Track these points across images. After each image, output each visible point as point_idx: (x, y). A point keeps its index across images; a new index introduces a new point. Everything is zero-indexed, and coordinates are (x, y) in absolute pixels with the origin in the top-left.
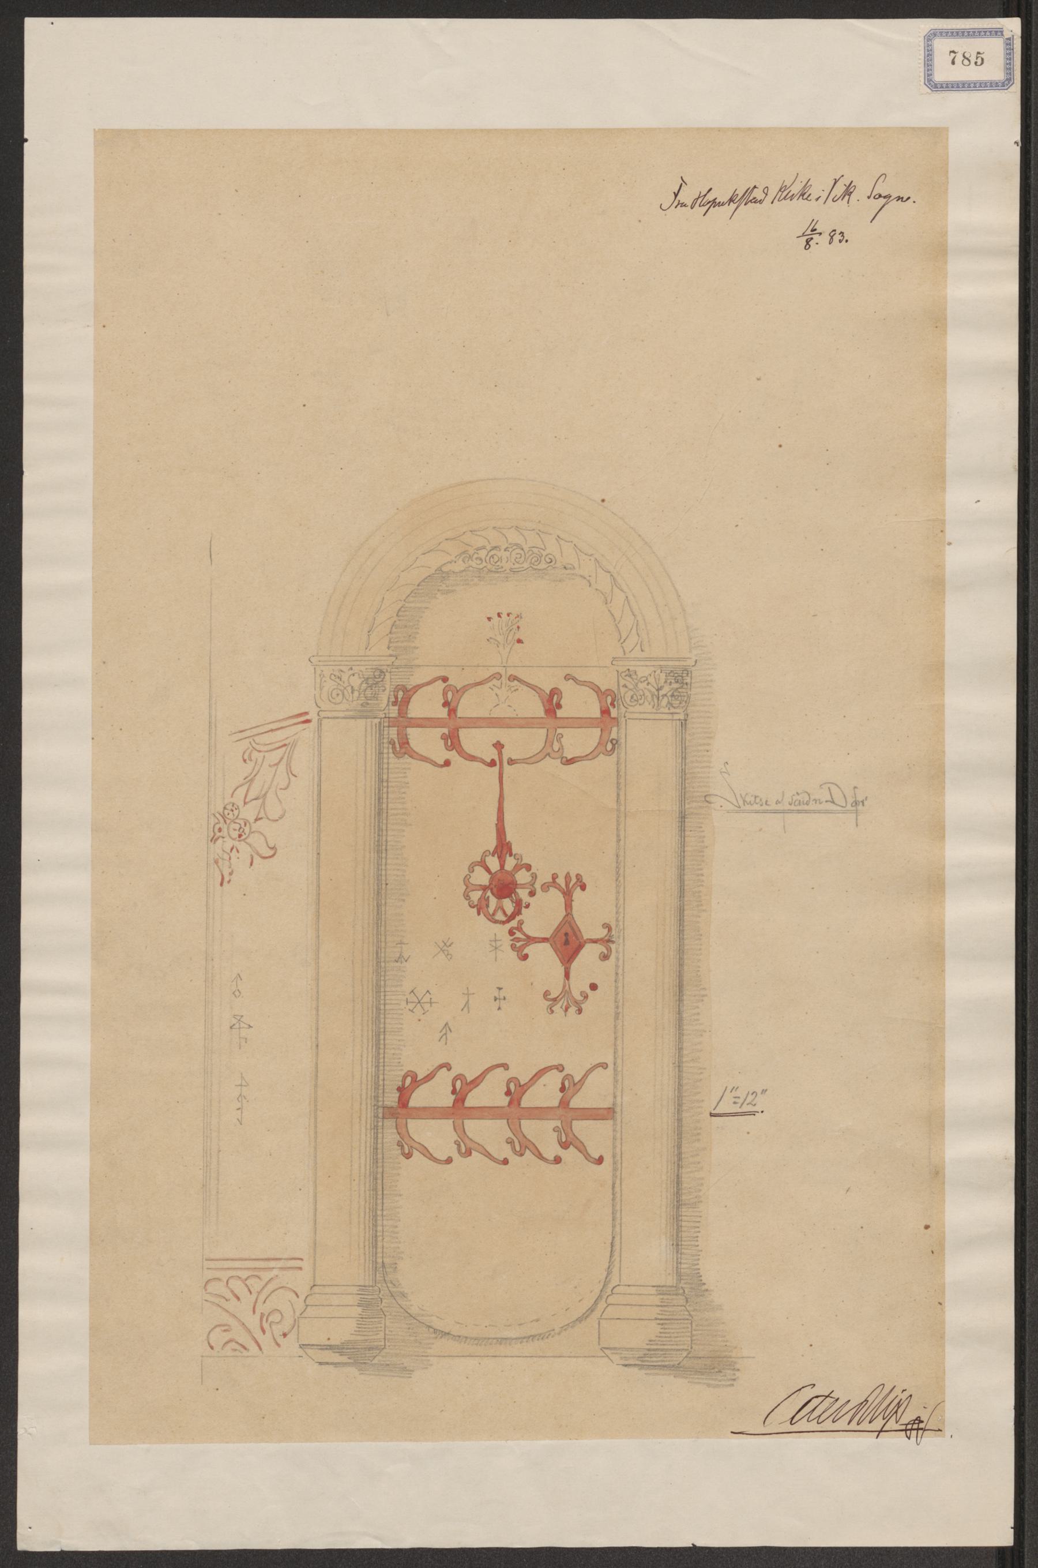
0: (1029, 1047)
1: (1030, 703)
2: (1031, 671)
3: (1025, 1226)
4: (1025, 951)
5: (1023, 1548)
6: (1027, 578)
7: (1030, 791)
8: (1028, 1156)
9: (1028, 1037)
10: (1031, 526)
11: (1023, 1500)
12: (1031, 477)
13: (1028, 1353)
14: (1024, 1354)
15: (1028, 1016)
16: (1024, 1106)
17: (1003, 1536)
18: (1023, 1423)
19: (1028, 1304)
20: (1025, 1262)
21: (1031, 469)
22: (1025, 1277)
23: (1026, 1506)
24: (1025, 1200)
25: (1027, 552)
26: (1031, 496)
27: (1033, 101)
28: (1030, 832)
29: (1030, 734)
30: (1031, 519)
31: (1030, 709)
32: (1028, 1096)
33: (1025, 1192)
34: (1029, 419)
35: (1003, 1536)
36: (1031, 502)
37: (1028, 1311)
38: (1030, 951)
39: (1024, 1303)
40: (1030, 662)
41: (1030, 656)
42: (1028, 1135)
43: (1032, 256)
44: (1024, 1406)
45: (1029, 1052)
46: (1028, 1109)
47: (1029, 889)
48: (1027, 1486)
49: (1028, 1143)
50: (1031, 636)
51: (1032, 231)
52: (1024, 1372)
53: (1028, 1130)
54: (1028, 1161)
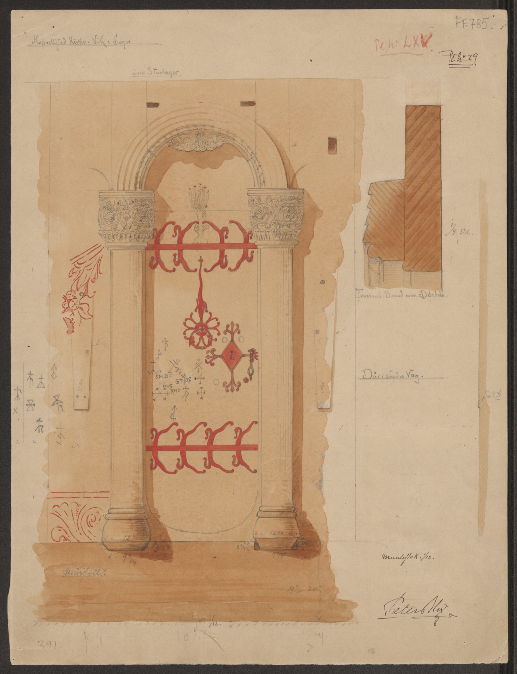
0: (515, 400)
1: (515, 220)
4: (512, 350)
5: (513, 661)
10: (515, 127)
15: (514, 383)
16: (513, 431)
18: (513, 596)
19: (515, 534)
20: (513, 512)
21: (515, 98)
22: (513, 520)
23: (515, 640)
24: (513, 479)
25: (513, 141)
26: (514, 112)
28: (515, 287)
29: (515, 236)
30: (515, 124)
31: (514, 223)
32: (514, 425)
33: (513, 475)
34: (513, 71)
36: (515, 115)
37: (515, 538)
39: (513, 533)
40: (515, 198)
41: (515, 196)
42: (514, 445)
44: (513, 587)
45: (514, 402)
46: (514, 432)
48: (515, 629)
49: (515, 450)
50: (515, 185)
52: (513, 569)
53: (514, 443)
54: (514, 459)
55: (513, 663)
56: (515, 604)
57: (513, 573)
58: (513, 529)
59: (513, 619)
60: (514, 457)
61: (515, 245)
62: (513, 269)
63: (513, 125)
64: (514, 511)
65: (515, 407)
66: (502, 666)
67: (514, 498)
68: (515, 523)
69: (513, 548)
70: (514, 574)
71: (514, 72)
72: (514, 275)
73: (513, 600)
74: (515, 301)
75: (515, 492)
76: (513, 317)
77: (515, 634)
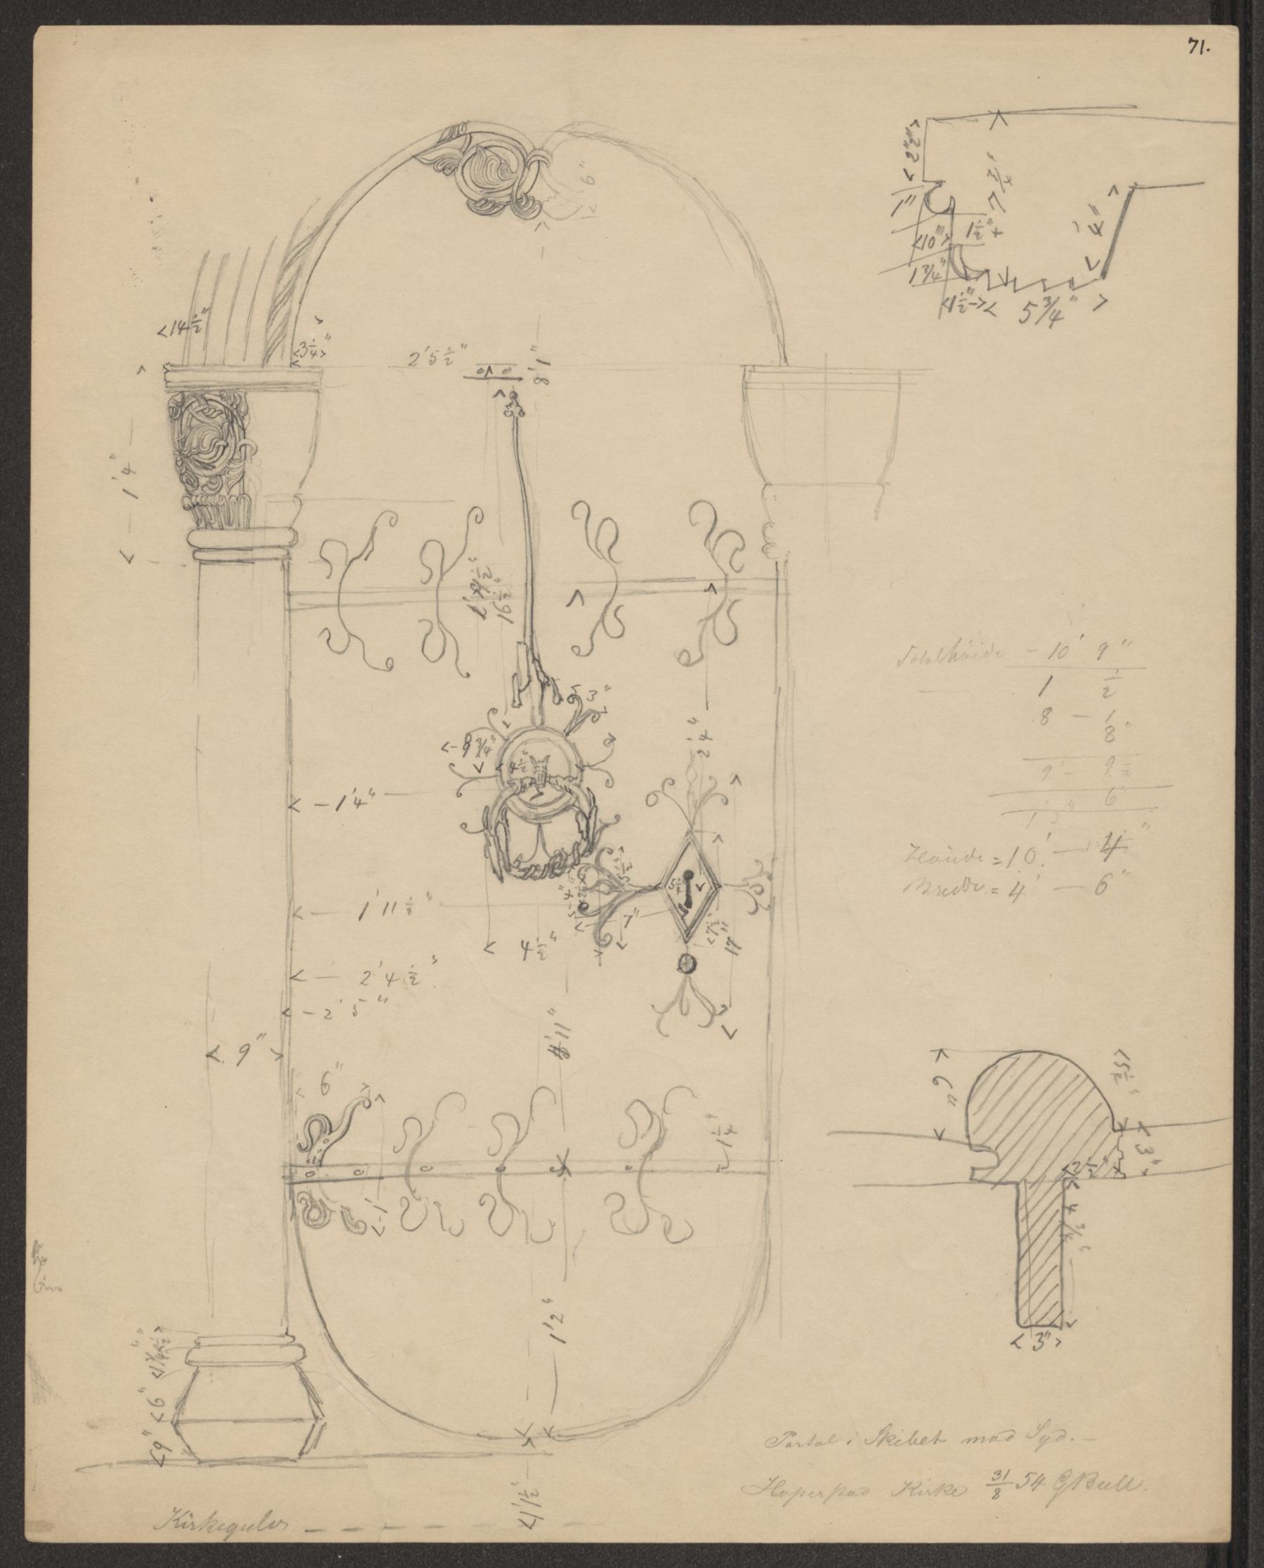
0: (1252, 841)
1: (1254, 342)
2: (1254, 296)
3: (1247, 1101)
7: (1253, 470)
8: (1252, 1000)
9: (1252, 826)
10: (1255, 85)
11: (1246, 1500)
13: (1252, 1286)
14: (1247, 1287)
15: (1251, 798)
18: (1246, 1388)
19: (1252, 1214)
23: (1251, 1509)
29: (1254, 386)
31: (1254, 351)
32: (1252, 911)
33: (1248, 1051)
36: (1254, 48)
37: (1252, 1224)
39: (1247, 1212)
45: (1252, 849)
47: (1254, 612)
48: (1252, 1479)
49: (1252, 981)
53: (1252, 962)
54: (1252, 1007)
56: (1251, 1408)
61: (1254, 411)
62: (1249, 479)
63: (1250, 78)
64: (1252, 1152)
65: (1252, 862)
66: (1212, 1549)
67: (1252, 1114)
68: (1252, 1185)
69: (1248, 1255)
70: (1251, 1326)
73: (1246, 1400)
75: (1251, 1099)
76: (1249, 613)
77: (1252, 1492)
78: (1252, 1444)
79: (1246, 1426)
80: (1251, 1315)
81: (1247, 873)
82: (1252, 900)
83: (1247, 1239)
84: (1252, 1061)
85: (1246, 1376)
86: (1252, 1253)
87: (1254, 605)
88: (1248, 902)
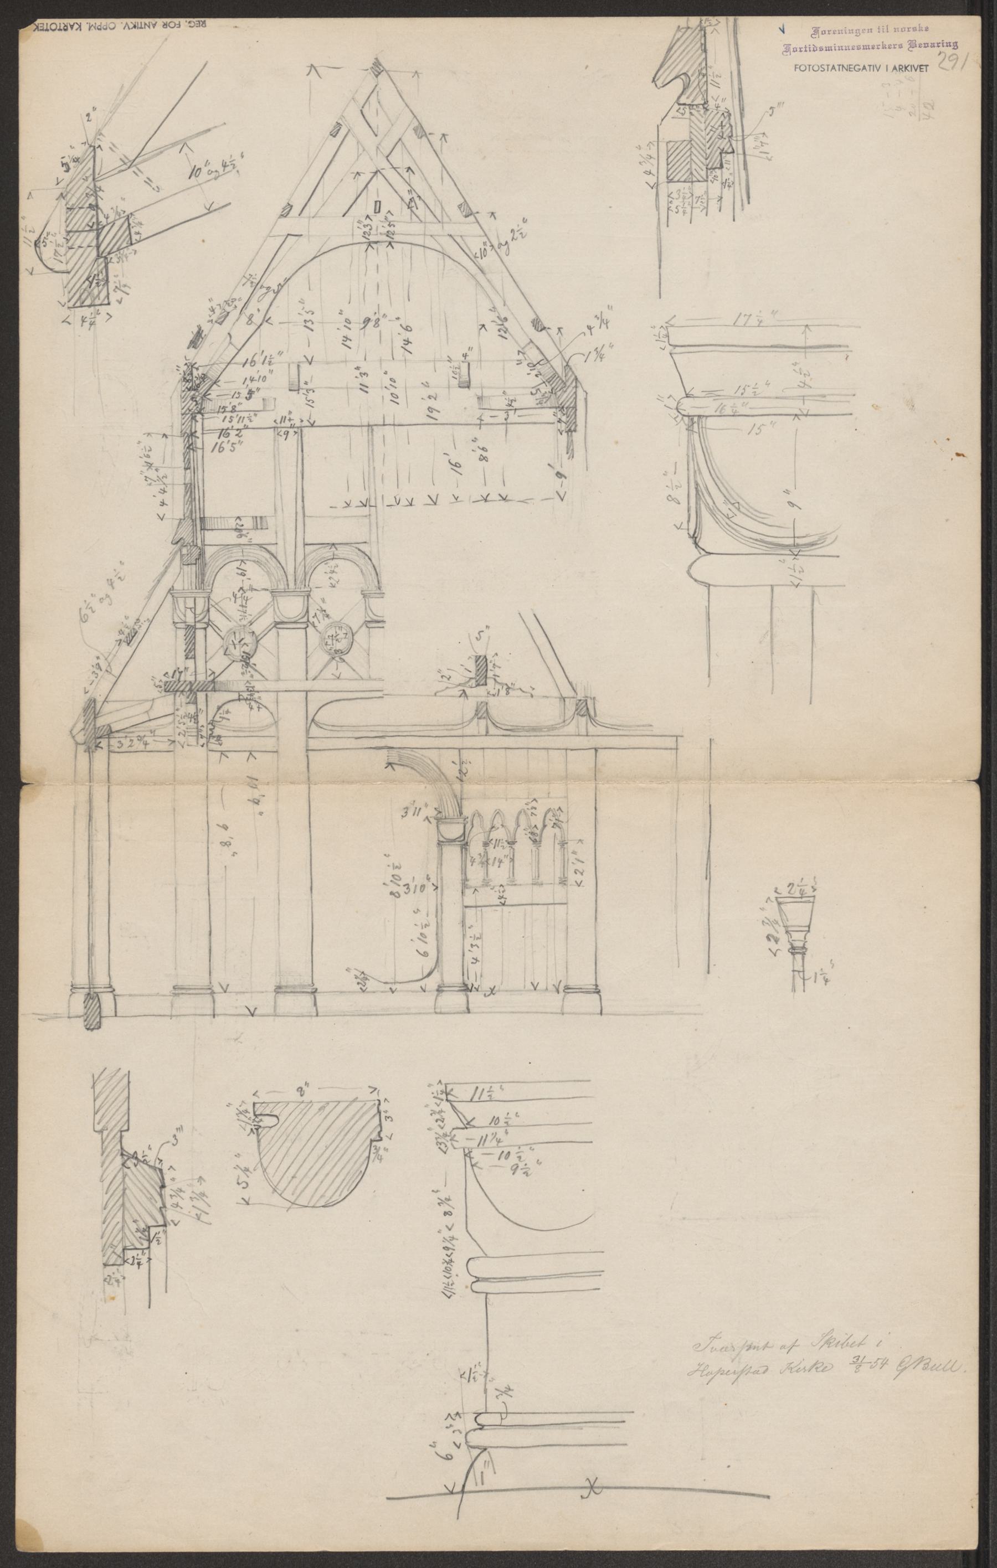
0: (992, 1044)
6: (990, 617)
10: (993, 570)
11: (988, 1457)
12: (993, 525)
14: (988, 1324)
15: (991, 1017)
17: (970, 1542)
18: (988, 1387)
19: (992, 1278)
21: (993, 519)
25: (990, 593)
27: (994, 183)
31: (993, 736)
35: (970, 1542)
36: (993, 548)
38: (992, 958)
43: (994, 323)
48: (991, 1444)
49: (992, 1132)
51: (994, 302)
55: (988, 1505)
56: (991, 1400)
57: (988, 1347)
58: (988, 1269)
59: (987, 1427)
60: (992, 1144)
65: (992, 1057)
71: (993, 474)
72: (992, 827)
74: (992, 872)
78: (992, 1422)
79: (988, 1411)
80: (991, 1341)
81: (989, 1064)
82: (991, 1081)
83: (989, 1293)
84: (992, 1182)
85: (988, 1379)
86: (991, 1303)
87: (993, 896)
88: (989, 1082)
